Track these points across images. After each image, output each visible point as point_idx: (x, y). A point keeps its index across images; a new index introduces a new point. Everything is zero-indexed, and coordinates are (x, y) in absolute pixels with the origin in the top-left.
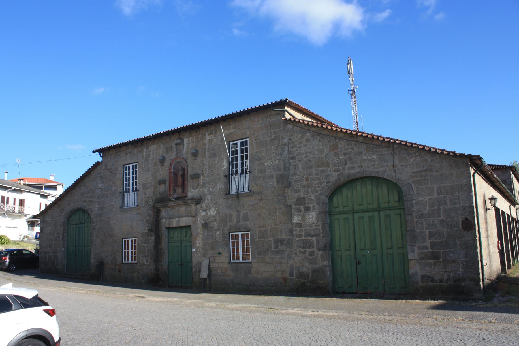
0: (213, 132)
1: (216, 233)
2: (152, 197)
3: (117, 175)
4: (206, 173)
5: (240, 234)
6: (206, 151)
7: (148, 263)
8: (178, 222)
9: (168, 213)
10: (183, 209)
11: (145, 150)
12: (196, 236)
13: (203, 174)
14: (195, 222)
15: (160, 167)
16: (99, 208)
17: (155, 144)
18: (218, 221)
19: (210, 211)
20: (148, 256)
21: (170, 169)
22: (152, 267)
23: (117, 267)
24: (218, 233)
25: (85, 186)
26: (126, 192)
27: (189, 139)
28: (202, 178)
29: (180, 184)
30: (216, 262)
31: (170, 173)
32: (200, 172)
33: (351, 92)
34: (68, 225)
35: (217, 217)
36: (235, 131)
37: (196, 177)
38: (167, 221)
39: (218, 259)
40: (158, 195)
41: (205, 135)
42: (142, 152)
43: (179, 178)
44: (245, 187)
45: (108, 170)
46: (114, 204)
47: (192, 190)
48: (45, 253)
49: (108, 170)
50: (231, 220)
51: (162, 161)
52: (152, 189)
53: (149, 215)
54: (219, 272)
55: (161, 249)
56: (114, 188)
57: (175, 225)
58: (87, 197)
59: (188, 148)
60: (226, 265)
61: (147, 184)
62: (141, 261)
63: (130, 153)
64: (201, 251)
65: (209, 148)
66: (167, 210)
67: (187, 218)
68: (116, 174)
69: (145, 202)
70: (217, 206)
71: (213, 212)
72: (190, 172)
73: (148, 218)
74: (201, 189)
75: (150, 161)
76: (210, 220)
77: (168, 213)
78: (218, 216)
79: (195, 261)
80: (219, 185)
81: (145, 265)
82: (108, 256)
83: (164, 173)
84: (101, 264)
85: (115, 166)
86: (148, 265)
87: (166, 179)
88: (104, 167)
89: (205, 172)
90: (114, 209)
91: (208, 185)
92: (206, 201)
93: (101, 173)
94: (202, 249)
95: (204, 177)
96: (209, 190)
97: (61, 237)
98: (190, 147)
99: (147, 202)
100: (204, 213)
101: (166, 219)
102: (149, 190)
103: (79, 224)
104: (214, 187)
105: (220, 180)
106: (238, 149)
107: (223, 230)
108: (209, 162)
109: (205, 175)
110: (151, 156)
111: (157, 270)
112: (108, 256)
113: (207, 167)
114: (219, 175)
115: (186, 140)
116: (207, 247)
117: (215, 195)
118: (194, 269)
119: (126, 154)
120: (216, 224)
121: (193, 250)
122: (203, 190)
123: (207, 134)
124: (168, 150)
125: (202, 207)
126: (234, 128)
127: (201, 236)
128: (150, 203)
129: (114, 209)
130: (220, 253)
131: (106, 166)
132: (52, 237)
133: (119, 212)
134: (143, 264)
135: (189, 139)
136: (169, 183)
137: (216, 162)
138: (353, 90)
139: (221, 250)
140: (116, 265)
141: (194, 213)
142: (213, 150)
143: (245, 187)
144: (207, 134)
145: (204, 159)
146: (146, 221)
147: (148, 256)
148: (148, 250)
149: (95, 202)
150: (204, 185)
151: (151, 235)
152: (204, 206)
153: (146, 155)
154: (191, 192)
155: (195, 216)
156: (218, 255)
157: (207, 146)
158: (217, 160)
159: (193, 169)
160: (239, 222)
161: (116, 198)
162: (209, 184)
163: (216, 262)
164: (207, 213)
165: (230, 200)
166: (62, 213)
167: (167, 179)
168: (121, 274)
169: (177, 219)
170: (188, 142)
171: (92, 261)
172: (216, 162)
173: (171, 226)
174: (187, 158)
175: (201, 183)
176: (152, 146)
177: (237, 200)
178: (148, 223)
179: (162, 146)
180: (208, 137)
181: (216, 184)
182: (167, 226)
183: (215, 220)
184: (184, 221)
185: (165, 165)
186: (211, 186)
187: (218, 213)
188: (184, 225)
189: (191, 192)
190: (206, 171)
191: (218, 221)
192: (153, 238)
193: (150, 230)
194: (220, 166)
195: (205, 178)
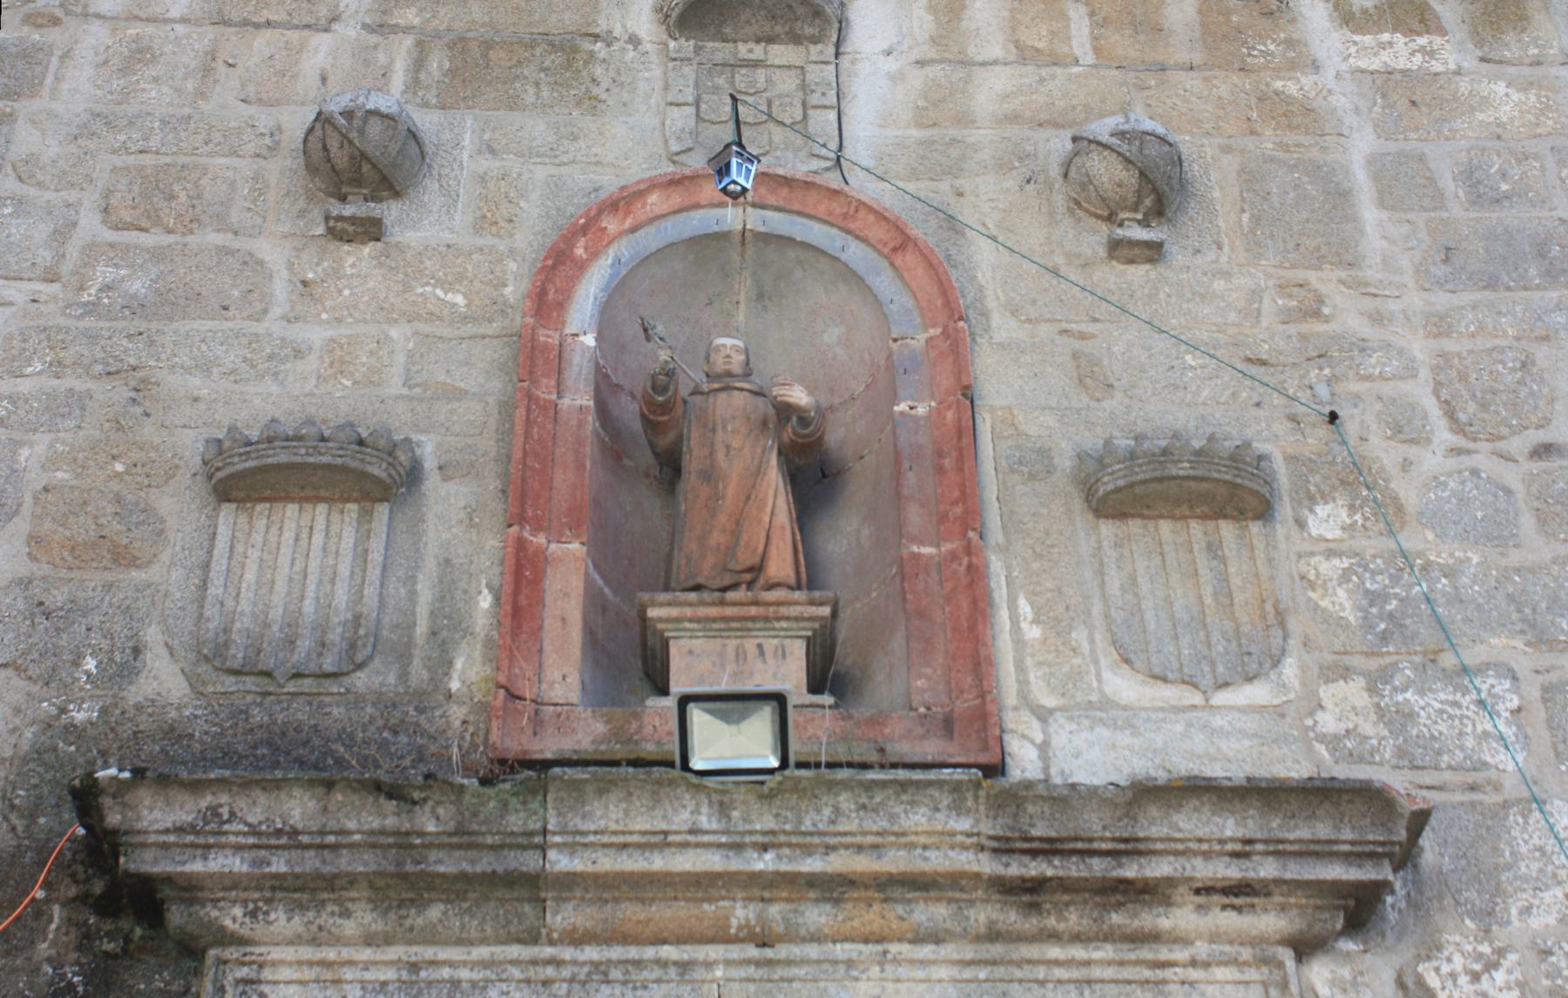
4: (1425, 469)
6: (1340, 197)
13: (1355, 479)
15: (272, 252)
21: (547, 300)
29: (781, 565)
31: (534, 358)
32: (1275, 441)
37: (1193, 488)
47: (1124, 687)
51: (358, 172)
72: (1026, 399)
74: (1353, 691)
87: (429, 450)
89: (1384, 452)
91: (1502, 645)
108: (1439, 325)
109: (1408, 492)
136: (524, 500)
145: (1325, 281)
150: (1406, 635)
154: (1102, 710)
157: (1359, 148)
159: (1090, 376)
162: (1541, 640)
175: (1342, 602)
189: (1102, 710)
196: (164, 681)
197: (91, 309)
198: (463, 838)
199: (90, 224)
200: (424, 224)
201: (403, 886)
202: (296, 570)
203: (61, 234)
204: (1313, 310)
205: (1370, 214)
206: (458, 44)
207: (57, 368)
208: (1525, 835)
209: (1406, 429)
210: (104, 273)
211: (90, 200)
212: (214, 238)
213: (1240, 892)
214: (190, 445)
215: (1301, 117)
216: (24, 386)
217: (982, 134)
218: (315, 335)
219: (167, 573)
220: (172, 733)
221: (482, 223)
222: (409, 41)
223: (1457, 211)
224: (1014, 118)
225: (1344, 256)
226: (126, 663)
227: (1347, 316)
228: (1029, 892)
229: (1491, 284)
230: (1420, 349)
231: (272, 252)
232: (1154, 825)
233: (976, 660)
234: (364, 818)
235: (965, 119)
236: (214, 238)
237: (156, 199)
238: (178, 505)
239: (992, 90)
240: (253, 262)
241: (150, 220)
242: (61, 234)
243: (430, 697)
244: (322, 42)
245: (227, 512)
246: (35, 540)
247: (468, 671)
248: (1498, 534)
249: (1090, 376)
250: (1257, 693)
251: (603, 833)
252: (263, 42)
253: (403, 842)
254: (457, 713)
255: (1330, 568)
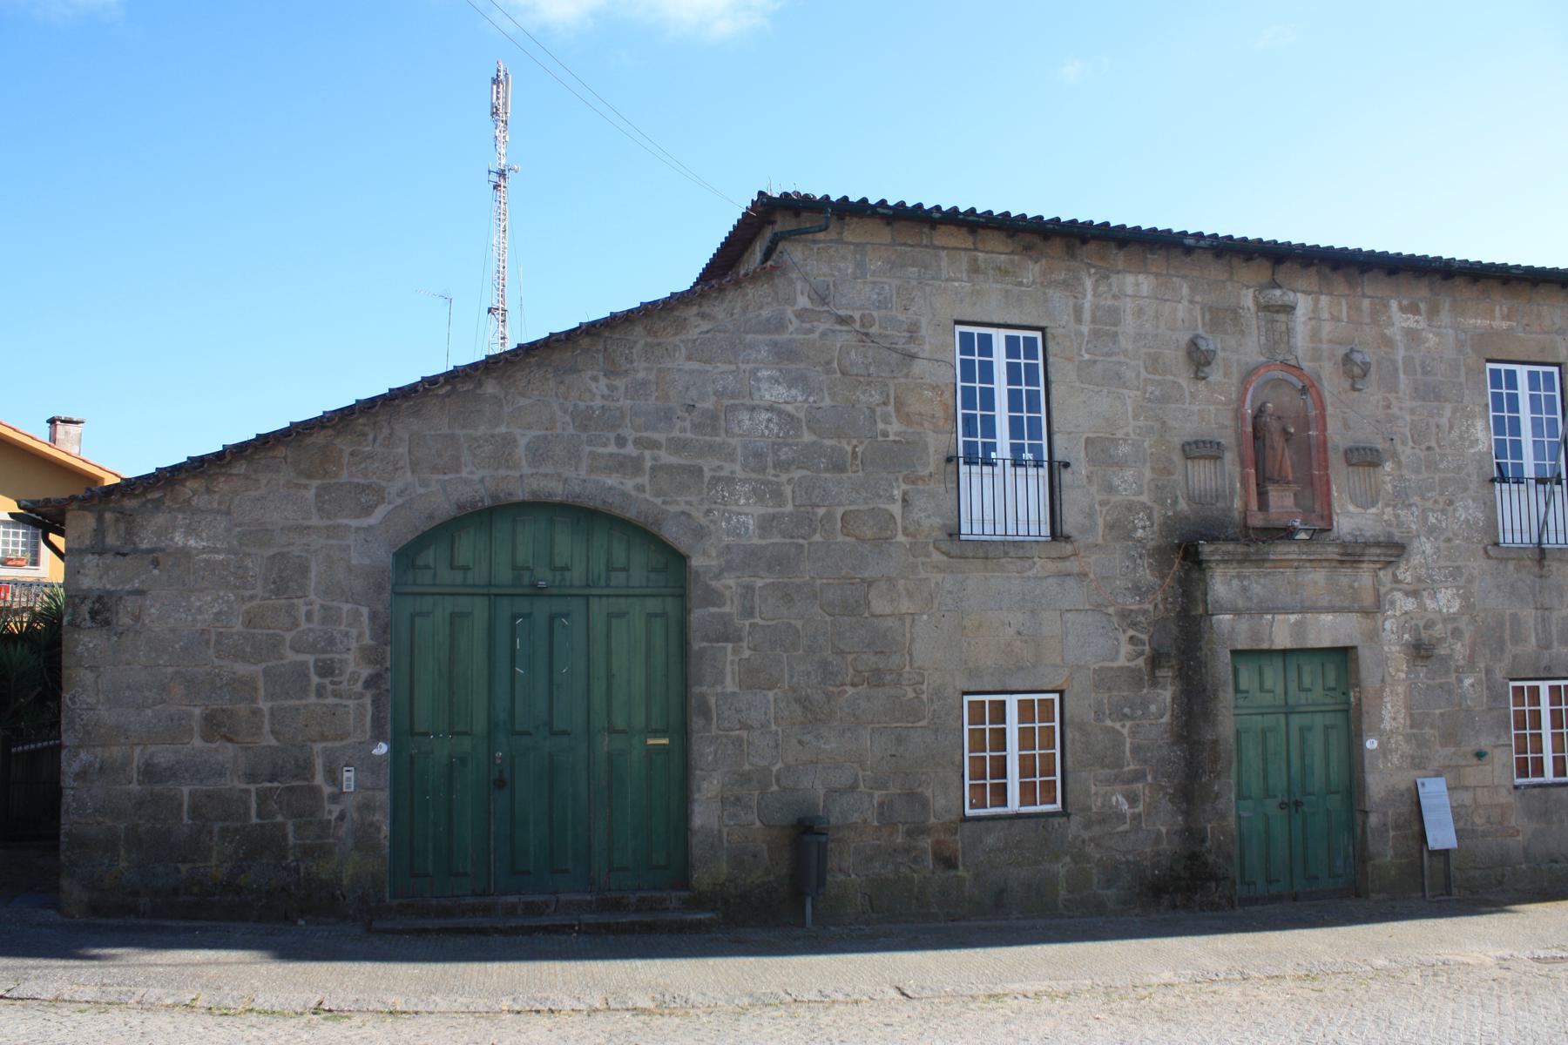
0: (1422, 306)
1: (1460, 681)
2: (1145, 507)
3: (918, 367)
4: (1406, 452)
5: (1544, 687)
6: (1396, 369)
7: (1140, 808)
8: (1299, 628)
9: (1244, 589)
10: (1316, 579)
11: (1089, 284)
12: (1382, 690)
13: (1394, 455)
14: (1374, 635)
15: (1184, 383)
16: (766, 524)
17: (1146, 272)
18: (1467, 637)
19: (1434, 597)
20: (1138, 776)
22: (1165, 823)
23: (926, 843)
24: (1467, 682)
25: (611, 373)
26: (970, 462)
27: (1316, 302)
28: (1388, 466)
30: (1466, 788)
31: (1239, 415)
32: (1380, 445)
33: (494, 178)
34: (396, 594)
35: (1463, 623)
36: (1511, 328)
37: (1365, 458)
38: (1243, 625)
39: (1475, 774)
40: (1183, 505)
41: (1387, 306)
42: (1072, 286)
43: (1281, 446)
44: (1517, 526)
45: (842, 321)
46: (896, 509)
47: (1351, 508)
48: (150, 773)
49: (842, 321)
50: (1517, 638)
52: (1148, 474)
53: (1136, 589)
54: (1478, 821)
55: (1215, 742)
56: (895, 427)
57: (1282, 641)
58: (654, 445)
59: (1315, 336)
60: (1504, 797)
61: (1115, 442)
62: (1096, 805)
63: (1004, 272)
64: (1406, 748)
65: (1408, 361)
66: (1240, 577)
67: (1341, 618)
68: (913, 357)
69: (1111, 527)
70: (1462, 582)
71: (1446, 601)
73: (1132, 603)
74: (1389, 510)
75: (1124, 343)
76: (1438, 630)
77: (1244, 589)
78: (1466, 618)
79: (1378, 784)
80: (1466, 508)
81: (1121, 817)
82: (853, 788)
83: (1209, 409)
84: (805, 836)
85: (902, 317)
86: (1136, 817)
88: (803, 302)
89: (1399, 448)
90: (901, 538)
91: (1416, 499)
92: (1416, 560)
93: (780, 326)
94: (1408, 739)
95: (1399, 464)
96: (1425, 519)
97: (355, 669)
98: (1324, 335)
99: (1120, 529)
100: (1409, 604)
101: (1237, 612)
102: (1129, 474)
103: (536, 592)
104: (1443, 511)
105: (1466, 489)
106: (1527, 392)
107: (1488, 671)
109: (1403, 459)
110: (1129, 324)
111: (1192, 834)
112: (853, 788)
113: (1407, 431)
114: (1460, 469)
115: (1303, 304)
116: (1428, 731)
117: (1449, 540)
118: (1373, 820)
119: (975, 269)
120: (1460, 650)
121: (1371, 744)
122: (1397, 516)
123: (1394, 304)
124: (1223, 317)
125: (1396, 580)
126: (1508, 317)
127: (1400, 689)
128: (1140, 533)
129: (901, 538)
130: (1480, 755)
131: (821, 297)
132: (242, 669)
133: (937, 557)
134: (1110, 817)
135: (1316, 302)
137: (1444, 421)
138: (502, 174)
139: (1484, 743)
140: (916, 831)
141: (1368, 600)
142: (1425, 373)
143: (1517, 526)
144: (1394, 304)
145: (1391, 396)
146: (1124, 615)
147: (1138, 776)
148: (1136, 749)
149: (730, 481)
150: (1401, 498)
151: (1154, 683)
152: (1405, 574)
153: (1096, 307)
154: (1348, 514)
155: (1374, 609)
156: (1475, 761)
157: (1401, 354)
158: (1448, 412)
159: (1346, 425)
160: (1548, 647)
161: (912, 480)
162: (1423, 498)
163: (1466, 788)
164: (1422, 606)
165: (1511, 566)
166: (367, 511)
167: (1227, 438)
168: (961, 872)
169: (1293, 618)
170: (1312, 313)
171: (704, 815)
172: (1444, 421)
173: (1265, 646)
174: (1320, 379)
175: (1389, 487)
176: (1130, 279)
177: (1536, 569)
178: (1134, 625)
179: (1185, 290)
180: (1400, 321)
181: (1451, 503)
182: (1242, 645)
183: (1457, 634)
184: (1327, 630)
185: (1212, 379)
186: (1429, 504)
187: (1467, 608)
188: (1326, 644)
189: (1348, 514)
190: (1404, 443)
191: (1467, 637)
192: (1167, 694)
193: (1155, 661)
194: (1461, 438)
195: (1407, 474)
196: (1183, 505)
197: (1149, 400)
198: (1257, 552)
199: (1143, 370)
200: (1215, 375)
201: (1245, 560)
202: (1202, 475)
203: (1138, 375)
204: (1388, 407)
205: (1402, 376)
206: (1210, 308)
207: (1146, 418)
208: (1416, 544)
209: (1404, 443)
210: (1150, 389)
211: (1141, 363)
212: (1170, 378)
213: (1374, 562)
214: (1177, 441)
215: (1388, 342)
216: (1141, 424)
217: (1325, 346)
218: (1195, 408)
219: (1178, 477)
220: (1187, 518)
221: (1226, 375)
222: (1198, 307)
223: (1419, 376)
224: (1330, 341)
225: (1394, 389)
226: (1175, 503)
227: (1395, 410)
228: (1341, 562)
229: (1423, 399)
230: (1408, 418)
231: (1184, 383)
232: (1368, 551)
233: (1328, 503)
234: (1241, 549)
235: (1320, 341)
236: (1170, 378)
237: (1155, 363)
238: (1177, 457)
239: (1327, 328)
240: (1180, 386)
241: (1155, 371)
242: (1138, 375)
243: (1230, 509)
244: (1180, 306)
245: (1189, 463)
246: (1153, 469)
247: (1237, 503)
248: (1418, 471)
249: (1346, 425)
250: (1373, 510)
251: (1282, 550)
252: (1167, 307)
253: (1247, 554)
254: (1236, 514)
255: (1388, 478)
